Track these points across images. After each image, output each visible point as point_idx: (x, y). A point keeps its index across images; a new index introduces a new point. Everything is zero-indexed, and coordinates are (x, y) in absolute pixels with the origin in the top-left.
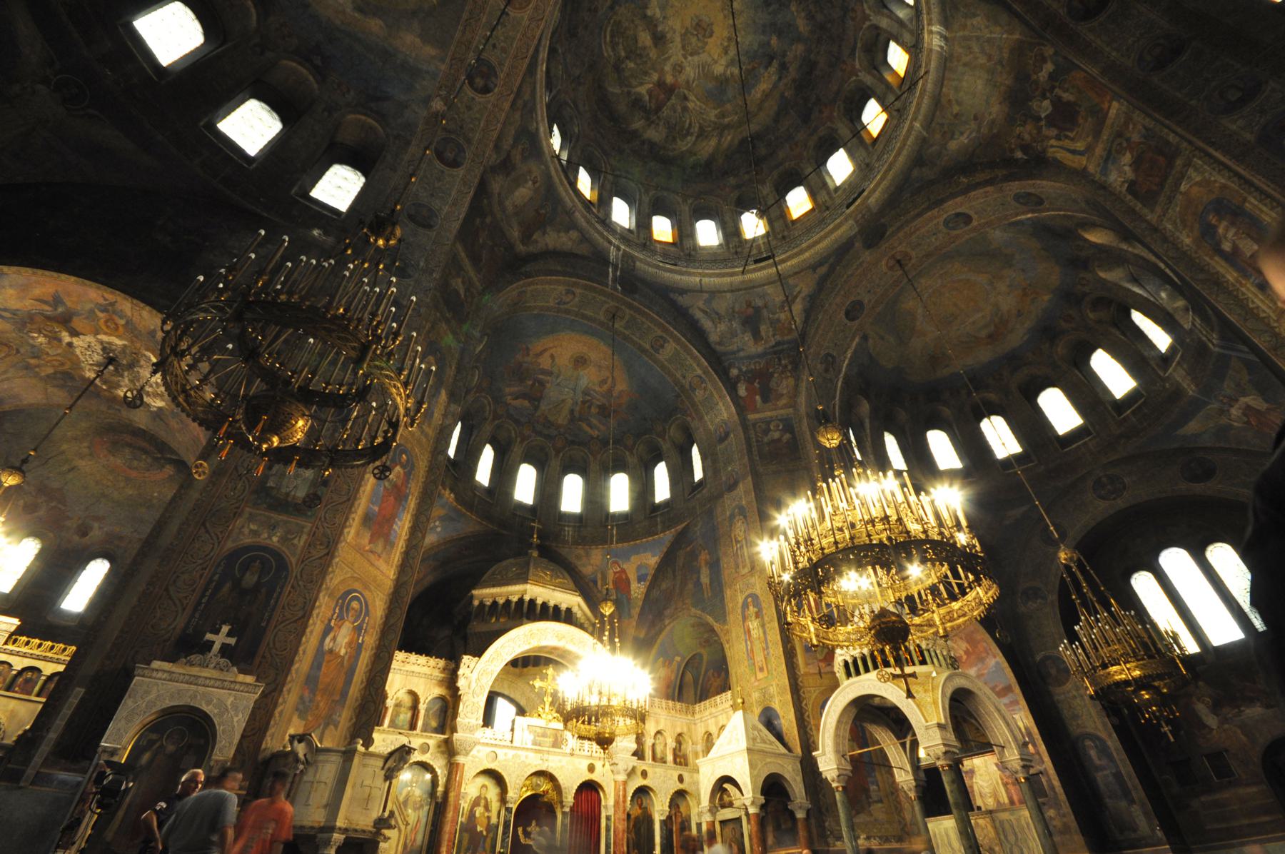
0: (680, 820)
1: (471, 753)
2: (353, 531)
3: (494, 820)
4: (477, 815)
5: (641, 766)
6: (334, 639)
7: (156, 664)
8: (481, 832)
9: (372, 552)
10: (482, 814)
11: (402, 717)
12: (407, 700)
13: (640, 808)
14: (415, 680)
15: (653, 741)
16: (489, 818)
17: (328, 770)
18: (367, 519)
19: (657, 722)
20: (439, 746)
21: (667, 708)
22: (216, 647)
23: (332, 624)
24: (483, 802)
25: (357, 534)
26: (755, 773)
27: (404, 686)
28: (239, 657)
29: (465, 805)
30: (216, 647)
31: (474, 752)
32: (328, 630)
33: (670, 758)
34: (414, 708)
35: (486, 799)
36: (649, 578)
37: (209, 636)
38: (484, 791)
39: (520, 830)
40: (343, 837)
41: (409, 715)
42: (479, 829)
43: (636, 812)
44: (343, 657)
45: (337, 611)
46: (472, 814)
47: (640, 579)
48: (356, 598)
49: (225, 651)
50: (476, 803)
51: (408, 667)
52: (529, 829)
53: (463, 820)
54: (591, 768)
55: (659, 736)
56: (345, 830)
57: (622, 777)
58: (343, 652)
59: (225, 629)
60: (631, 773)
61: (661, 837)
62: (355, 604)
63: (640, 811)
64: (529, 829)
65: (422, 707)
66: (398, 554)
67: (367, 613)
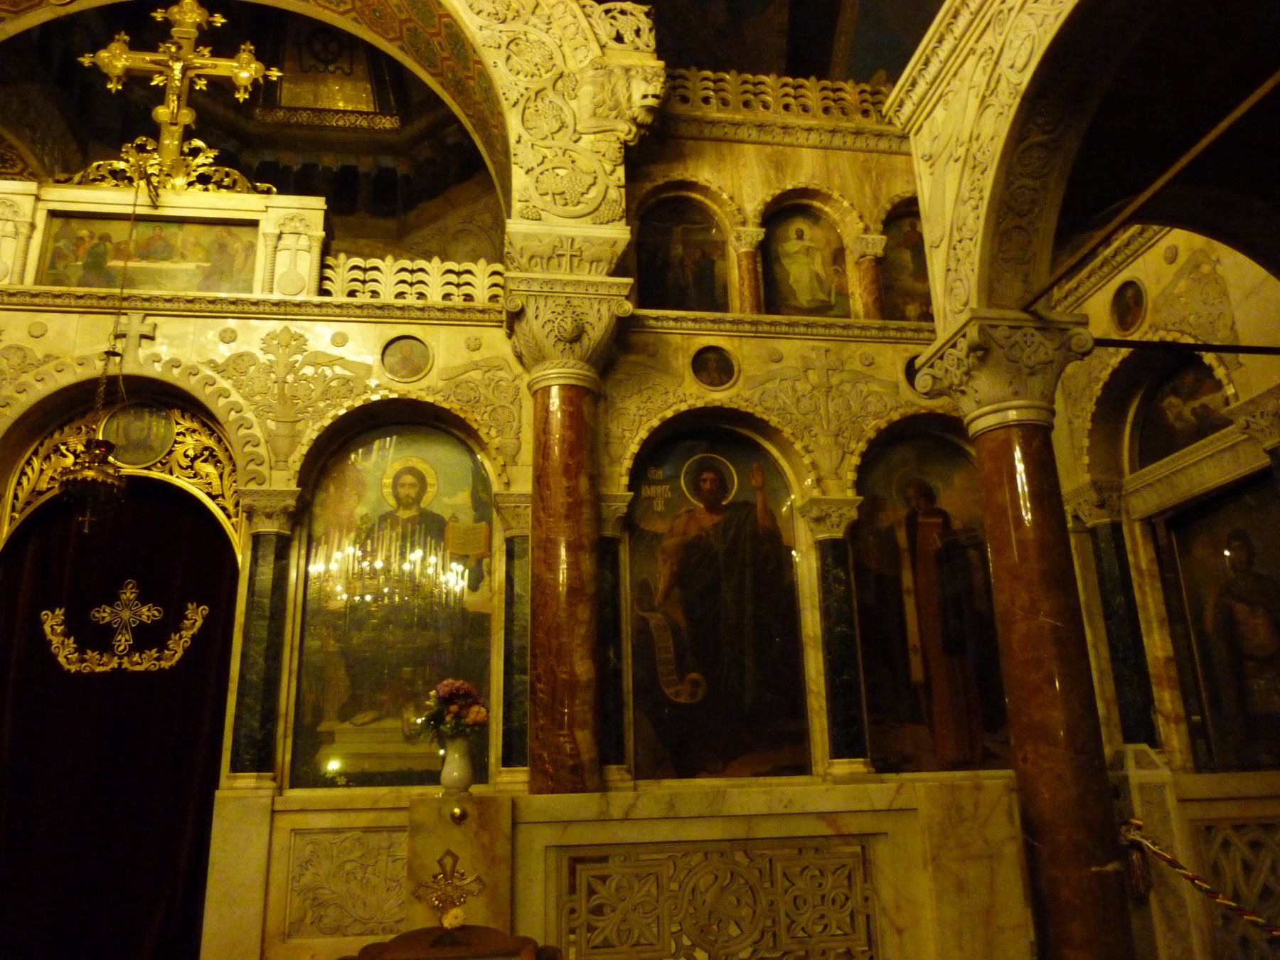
0: (936, 542)
13: (712, 507)
15: (754, 233)
19: (779, 166)
33: (859, 296)
39: (52, 622)
52: (104, 614)
61: (826, 613)
63: (708, 520)
64: (104, 614)
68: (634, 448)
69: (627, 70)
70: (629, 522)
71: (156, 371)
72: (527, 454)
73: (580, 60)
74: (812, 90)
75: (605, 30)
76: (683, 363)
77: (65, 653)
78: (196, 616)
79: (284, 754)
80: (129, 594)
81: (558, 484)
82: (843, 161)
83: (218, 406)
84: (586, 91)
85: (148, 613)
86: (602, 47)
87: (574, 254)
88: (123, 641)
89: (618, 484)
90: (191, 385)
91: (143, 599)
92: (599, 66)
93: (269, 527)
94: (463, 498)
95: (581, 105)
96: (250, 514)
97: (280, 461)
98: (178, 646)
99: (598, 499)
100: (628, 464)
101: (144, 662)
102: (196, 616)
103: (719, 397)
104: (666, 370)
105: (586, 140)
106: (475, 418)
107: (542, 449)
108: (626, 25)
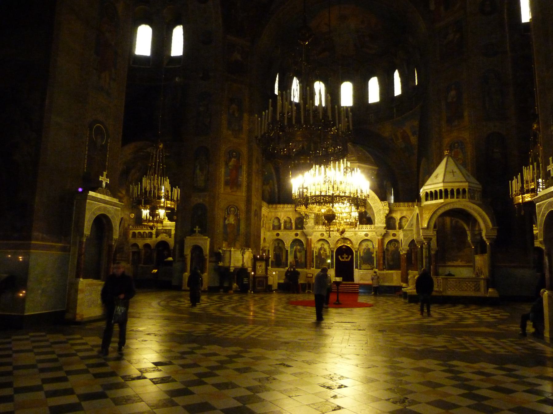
1: (314, 234)
2: (222, 189)
3: (328, 254)
4: (322, 253)
5: (391, 232)
6: (229, 220)
7: (187, 237)
8: (324, 258)
9: (232, 192)
10: (323, 253)
11: (288, 225)
12: (288, 220)
13: (394, 246)
14: (288, 213)
15: (399, 221)
16: (326, 254)
17: (227, 255)
18: (227, 183)
19: (402, 213)
20: (302, 234)
21: (409, 206)
22: (197, 232)
23: (226, 216)
24: (323, 249)
25: (224, 189)
26: (406, 238)
27: (285, 216)
28: (204, 232)
29: (315, 250)
30: (197, 232)
31: (315, 234)
32: (225, 219)
34: (291, 222)
35: (324, 248)
36: (417, 133)
37: (195, 229)
38: (323, 246)
39: (339, 257)
40: (233, 268)
41: (290, 225)
42: (323, 257)
43: (392, 248)
44: (234, 224)
45: (226, 213)
46: (319, 253)
47: (414, 134)
48: (232, 207)
49: (199, 232)
50: (321, 249)
51: (285, 209)
52: (343, 256)
53: (317, 254)
54: (366, 235)
55: (404, 218)
56: (234, 267)
57: (380, 238)
58: (233, 223)
59: (197, 227)
60: (385, 235)
62: (232, 209)
64: (343, 256)
65: (293, 222)
66: (244, 188)
67: (238, 210)
68: (387, 243)
69: (385, 209)
70: (387, 249)
71: (346, 237)
72: (377, 244)
73: (381, 208)
74: (406, 204)
75: (384, 205)
76: (391, 235)
77: (341, 259)
78: (350, 256)
79: (359, 267)
80: (345, 254)
81: (380, 247)
82: (409, 212)
83: (352, 240)
84: (382, 211)
85: (347, 256)
86: (383, 207)
87: (381, 227)
88: (345, 258)
89: (385, 246)
90: (349, 238)
91: (346, 255)
92: (384, 209)
93: (356, 250)
94: (372, 246)
95: (381, 212)
96: (355, 249)
97: (357, 245)
98: (349, 259)
99: (383, 248)
100: (386, 244)
101: (347, 260)
102: (350, 256)
103: (394, 238)
104: (389, 236)
105: (382, 216)
106: (372, 240)
107: (379, 244)
108: (386, 204)
